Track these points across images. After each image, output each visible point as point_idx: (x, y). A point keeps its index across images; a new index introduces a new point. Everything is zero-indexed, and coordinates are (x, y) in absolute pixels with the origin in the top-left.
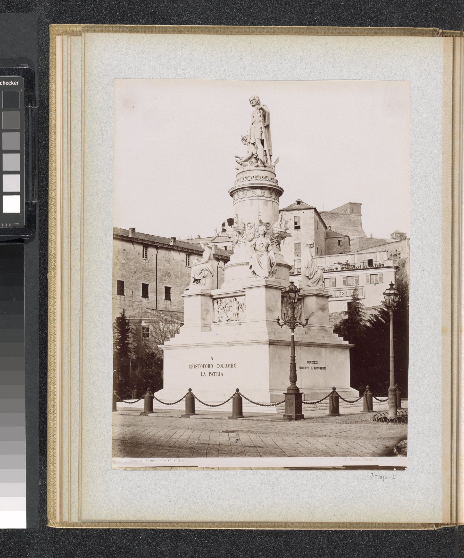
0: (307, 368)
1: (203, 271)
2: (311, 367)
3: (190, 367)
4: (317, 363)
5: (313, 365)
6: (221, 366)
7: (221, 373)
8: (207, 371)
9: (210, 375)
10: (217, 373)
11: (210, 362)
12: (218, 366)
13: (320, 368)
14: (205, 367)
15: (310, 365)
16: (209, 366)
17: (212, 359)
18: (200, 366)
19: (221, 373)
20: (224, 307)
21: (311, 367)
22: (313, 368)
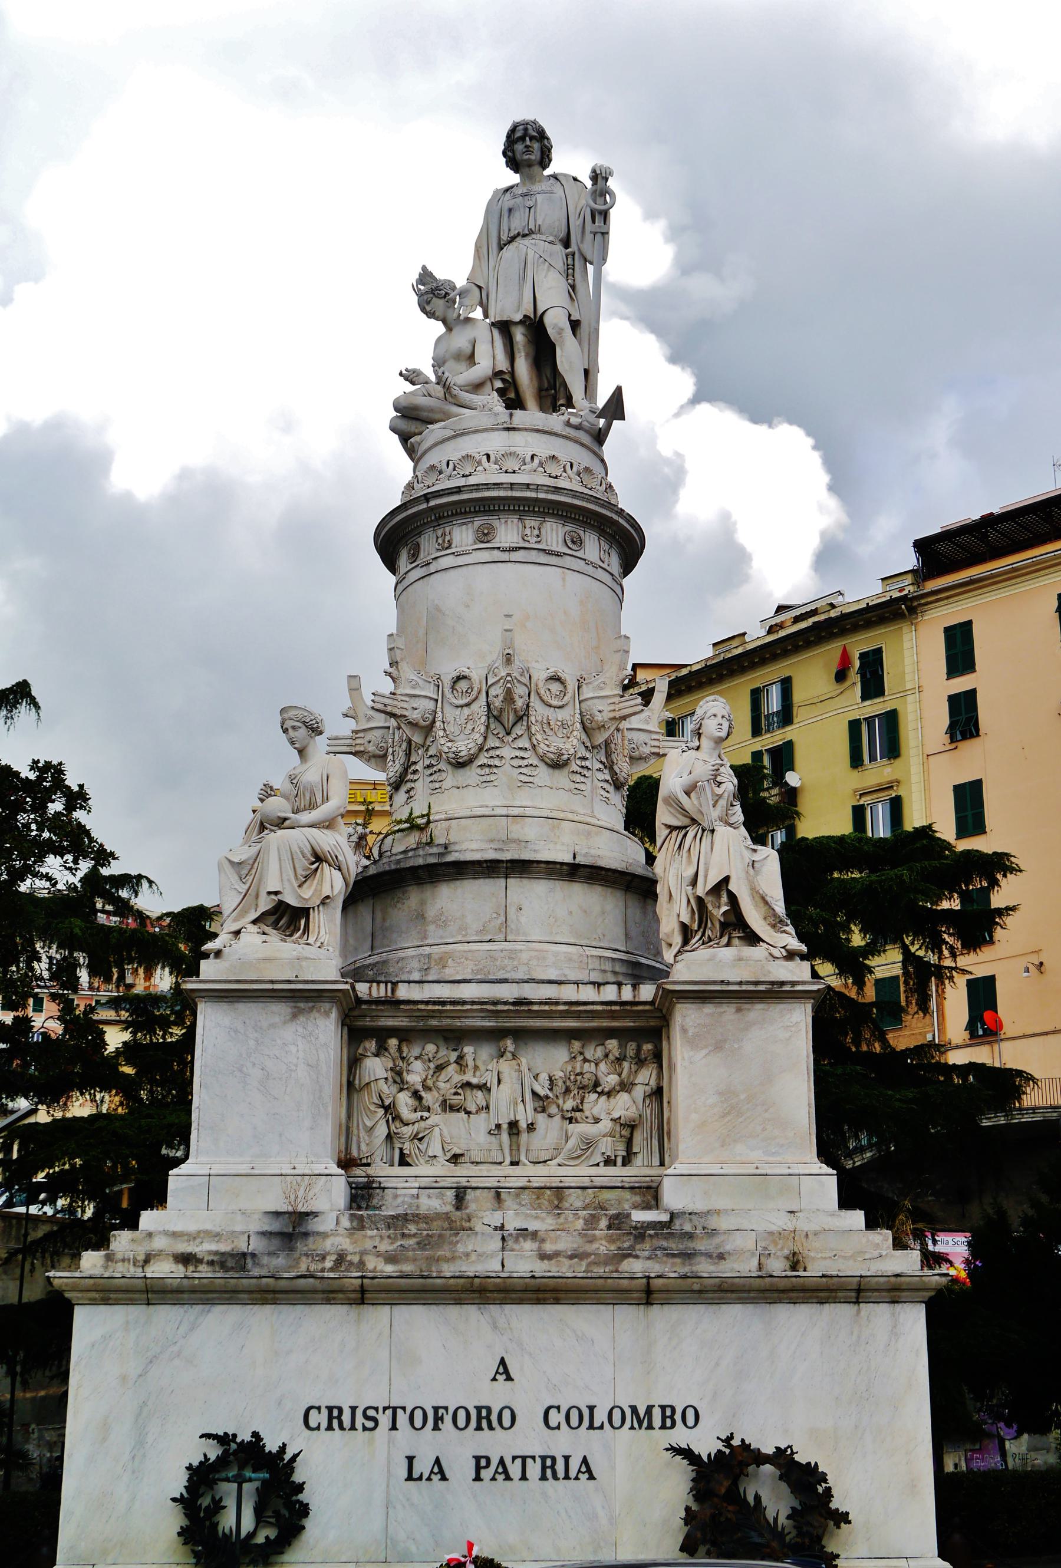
3: (318, 1418)
7: (575, 1465)
9: (486, 1474)
10: (548, 1467)
11: (496, 1396)
17: (504, 1369)
18: (402, 1418)
19: (575, 1465)
20: (430, 1083)
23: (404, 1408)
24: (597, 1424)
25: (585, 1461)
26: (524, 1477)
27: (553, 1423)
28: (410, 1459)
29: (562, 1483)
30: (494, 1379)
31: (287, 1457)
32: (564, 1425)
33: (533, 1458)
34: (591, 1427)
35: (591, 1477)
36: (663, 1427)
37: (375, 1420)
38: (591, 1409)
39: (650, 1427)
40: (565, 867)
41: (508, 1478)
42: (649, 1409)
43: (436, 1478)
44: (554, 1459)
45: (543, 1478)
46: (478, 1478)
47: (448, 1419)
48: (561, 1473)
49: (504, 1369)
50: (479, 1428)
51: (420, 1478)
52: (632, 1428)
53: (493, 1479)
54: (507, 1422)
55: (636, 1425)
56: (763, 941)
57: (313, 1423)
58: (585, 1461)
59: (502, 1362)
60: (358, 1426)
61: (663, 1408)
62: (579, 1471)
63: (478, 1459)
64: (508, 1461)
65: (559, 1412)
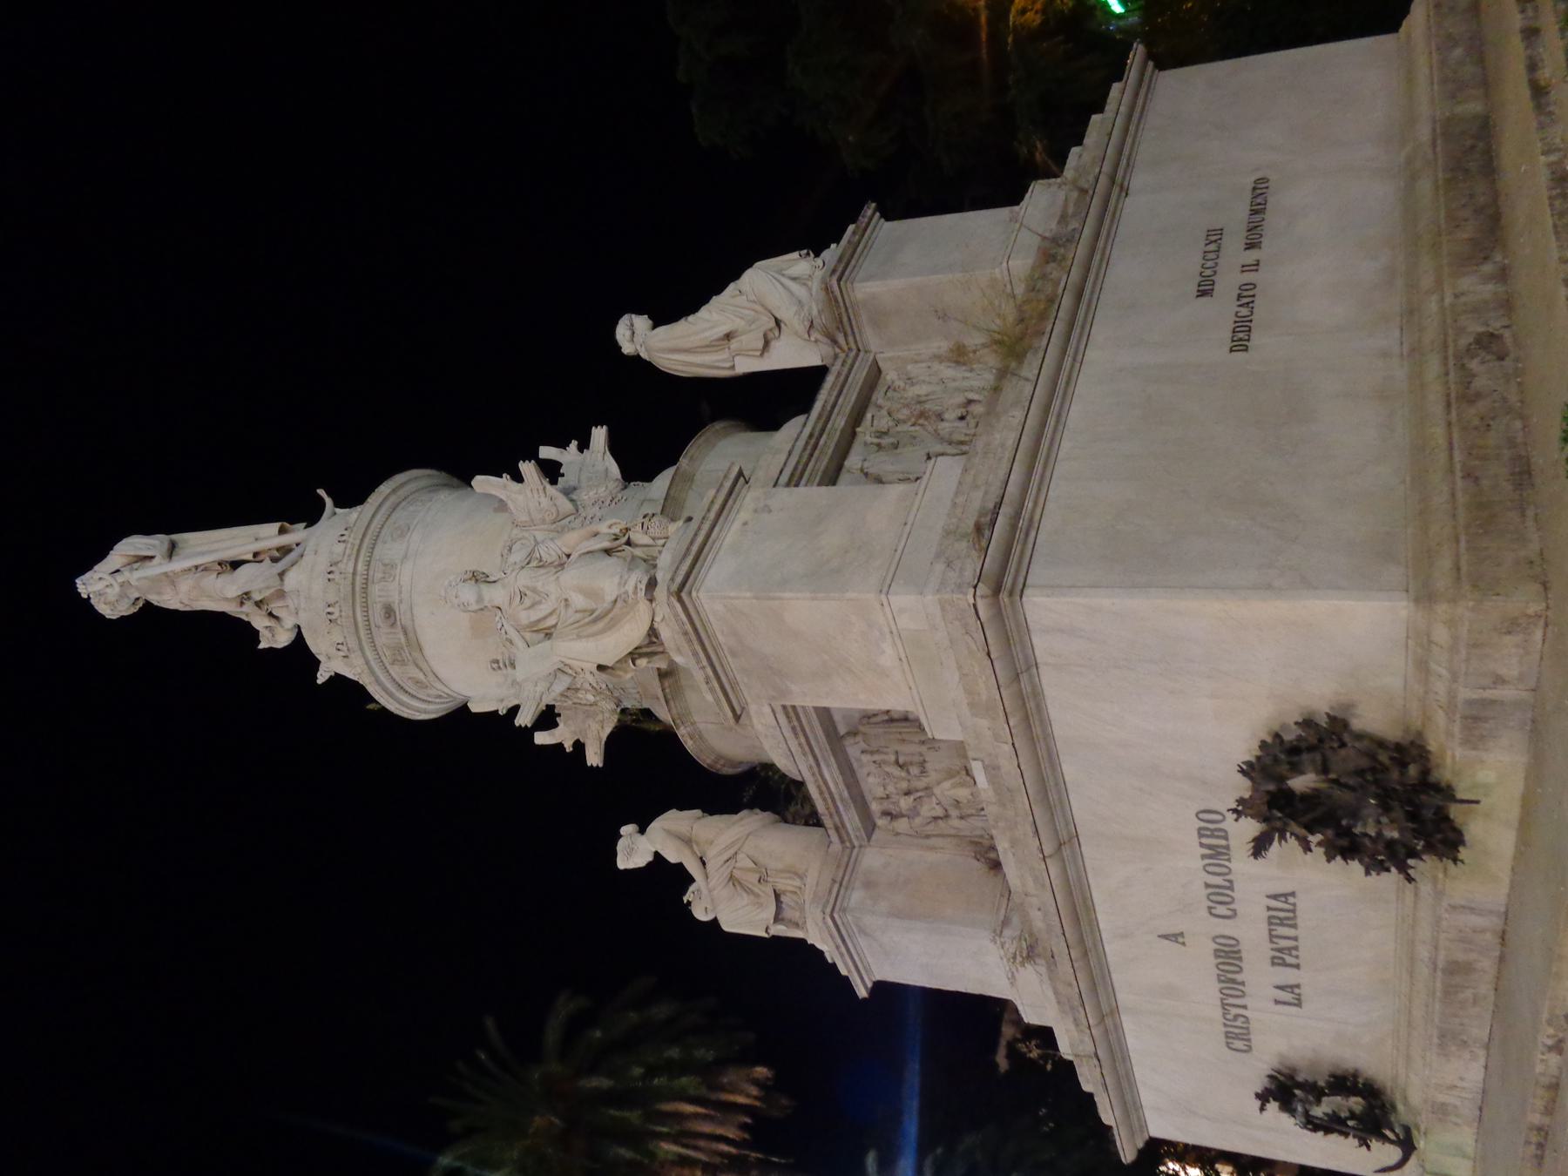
0: (1246, 296)
1: (737, 873)
2: (1245, 268)
4: (1215, 237)
5: (1234, 252)
6: (1221, 897)
7: (1274, 903)
8: (1260, 977)
9: (1289, 960)
12: (1221, 910)
13: (1254, 212)
14: (1239, 977)
15: (1229, 282)
16: (1228, 955)
17: (1175, 937)
19: (1274, 903)
20: (904, 785)
21: (1245, 268)
22: (1252, 256)
23: (1222, 999)
24: (1227, 884)
25: (1275, 897)
26: (1295, 939)
27: (1229, 913)
28: (1277, 1002)
29: (1297, 913)
30: (1184, 944)
31: (1281, 1078)
32: (1232, 906)
33: (1270, 930)
34: (1231, 888)
35: (1293, 894)
36: (1226, 838)
37: (1236, 1017)
38: (1207, 886)
39: (1227, 847)
40: (666, 684)
41: (1296, 948)
42: (1202, 845)
43: (1297, 991)
44: (1270, 917)
45: (1294, 926)
46: (1297, 966)
47: (1230, 976)
48: (1291, 915)
49: (1175, 937)
50: (1240, 959)
51: (1299, 1000)
52: (1229, 860)
53: (1297, 957)
54: (1233, 942)
55: (1226, 857)
56: (652, 624)
57: (1245, 1048)
58: (1268, 897)
59: (1166, 937)
60: (1244, 1025)
61: (1201, 836)
62: (1286, 902)
63: (1273, 964)
64: (1275, 946)
65: (1214, 908)
